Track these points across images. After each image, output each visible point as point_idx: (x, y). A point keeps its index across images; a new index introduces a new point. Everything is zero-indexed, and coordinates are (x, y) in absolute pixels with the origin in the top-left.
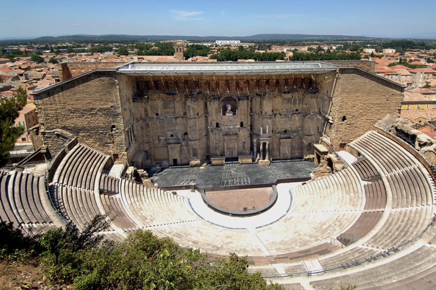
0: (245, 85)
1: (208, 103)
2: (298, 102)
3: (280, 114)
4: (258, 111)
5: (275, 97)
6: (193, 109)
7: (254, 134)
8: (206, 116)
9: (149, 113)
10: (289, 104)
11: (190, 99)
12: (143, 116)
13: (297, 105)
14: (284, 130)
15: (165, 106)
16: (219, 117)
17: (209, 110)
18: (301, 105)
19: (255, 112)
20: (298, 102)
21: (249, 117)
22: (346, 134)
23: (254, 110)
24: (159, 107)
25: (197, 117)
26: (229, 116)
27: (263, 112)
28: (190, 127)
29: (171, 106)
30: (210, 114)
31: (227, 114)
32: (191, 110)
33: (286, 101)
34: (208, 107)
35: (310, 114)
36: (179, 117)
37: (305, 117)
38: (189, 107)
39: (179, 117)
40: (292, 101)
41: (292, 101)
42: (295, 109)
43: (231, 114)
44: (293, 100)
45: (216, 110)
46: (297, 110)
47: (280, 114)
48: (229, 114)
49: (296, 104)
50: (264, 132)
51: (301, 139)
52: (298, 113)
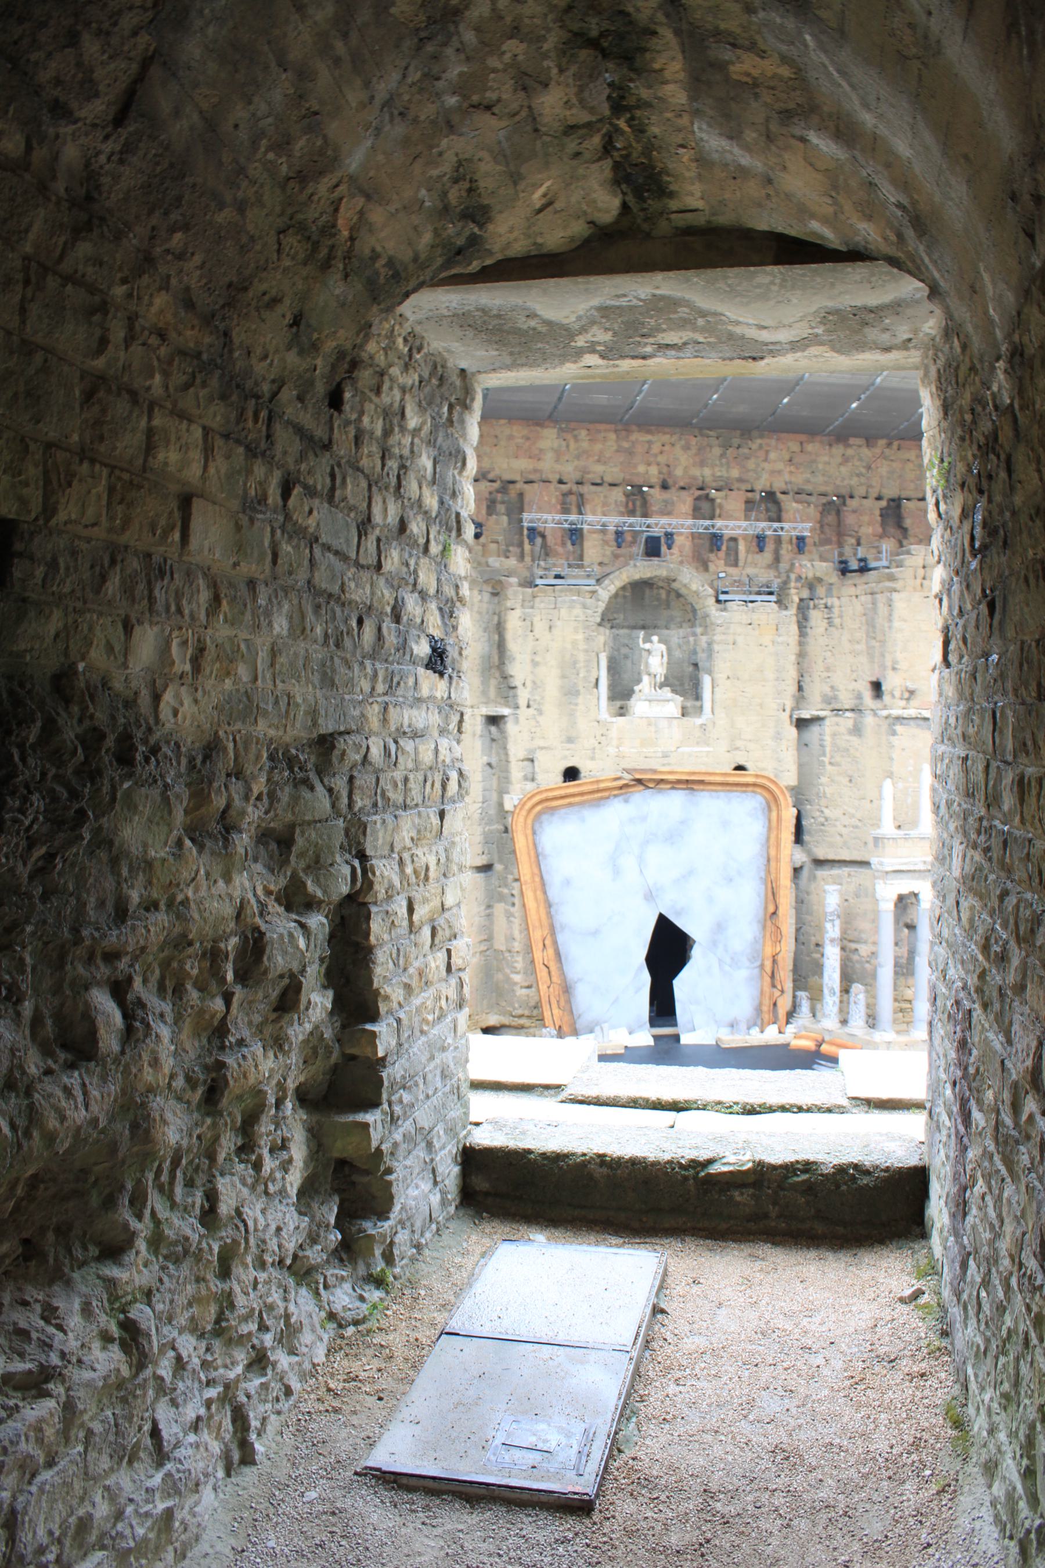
1: (513, 622)
4: (851, 685)
7: (819, 863)
16: (583, 725)
17: (519, 670)
23: (816, 690)
26: (650, 722)
27: (892, 683)
30: (523, 696)
34: (513, 645)
45: (568, 667)
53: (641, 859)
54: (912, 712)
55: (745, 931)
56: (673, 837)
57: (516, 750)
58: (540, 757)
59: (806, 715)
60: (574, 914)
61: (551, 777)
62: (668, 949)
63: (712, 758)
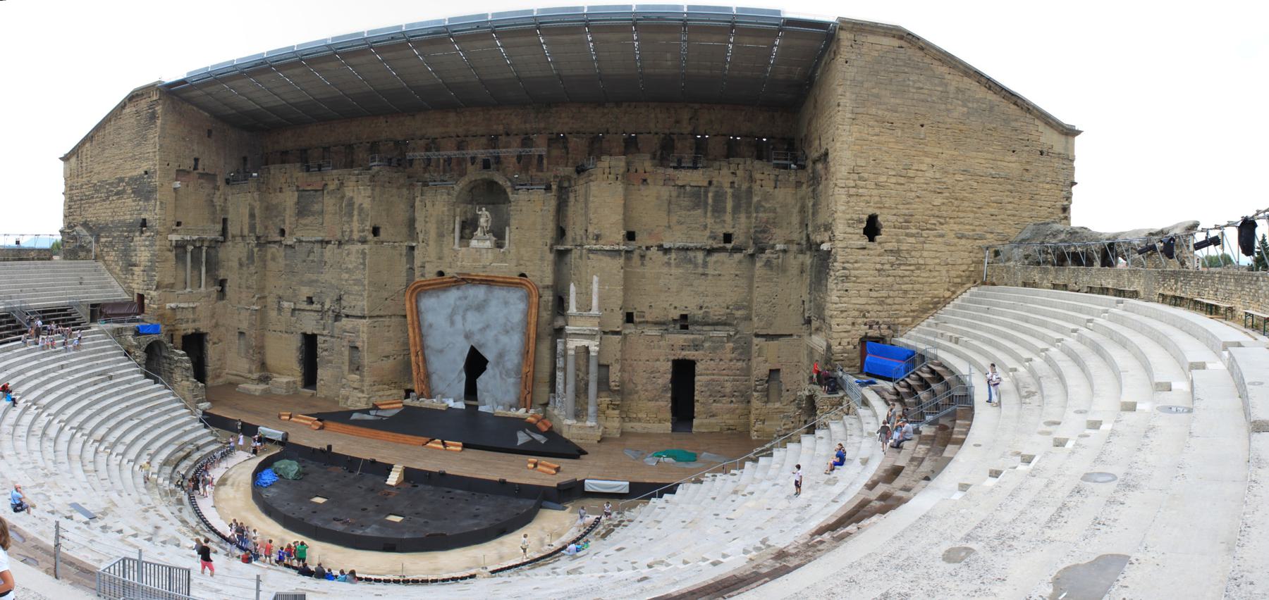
0: (555, 152)
1: (417, 203)
2: (729, 205)
3: (660, 247)
5: (645, 180)
6: (361, 210)
8: (412, 248)
9: (258, 220)
10: (699, 212)
11: (354, 178)
12: (246, 232)
13: (728, 217)
14: (676, 314)
15: (302, 211)
16: (446, 251)
17: (419, 226)
18: (743, 218)
19: (574, 240)
20: (729, 205)
21: (550, 257)
22: (884, 293)
23: (570, 234)
24: (288, 212)
25: (370, 237)
26: (478, 250)
28: (348, 271)
29: (316, 207)
30: (421, 237)
31: (474, 243)
32: (356, 213)
33: (686, 202)
35: (773, 247)
36: (328, 242)
37: (753, 263)
38: (351, 204)
39: (328, 242)
40: (710, 201)
41: (710, 201)
42: (720, 232)
43: (488, 244)
44: (710, 195)
45: (440, 223)
46: (728, 238)
47: (660, 247)
48: (481, 243)
49: (724, 210)
50: (585, 306)
51: (744, 351)
52: (737, 250)
53: (464, 318)
54: (597, 247)
55: (513, 359)
56: (480, 307)
57: (417, 263)
58: (427, 265)
59: (561, 248)
60: (434, 341)
61: (431, 274)
62: (476, 364)
63: (505, 268)
